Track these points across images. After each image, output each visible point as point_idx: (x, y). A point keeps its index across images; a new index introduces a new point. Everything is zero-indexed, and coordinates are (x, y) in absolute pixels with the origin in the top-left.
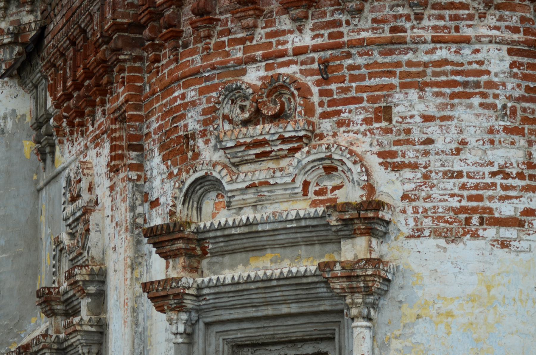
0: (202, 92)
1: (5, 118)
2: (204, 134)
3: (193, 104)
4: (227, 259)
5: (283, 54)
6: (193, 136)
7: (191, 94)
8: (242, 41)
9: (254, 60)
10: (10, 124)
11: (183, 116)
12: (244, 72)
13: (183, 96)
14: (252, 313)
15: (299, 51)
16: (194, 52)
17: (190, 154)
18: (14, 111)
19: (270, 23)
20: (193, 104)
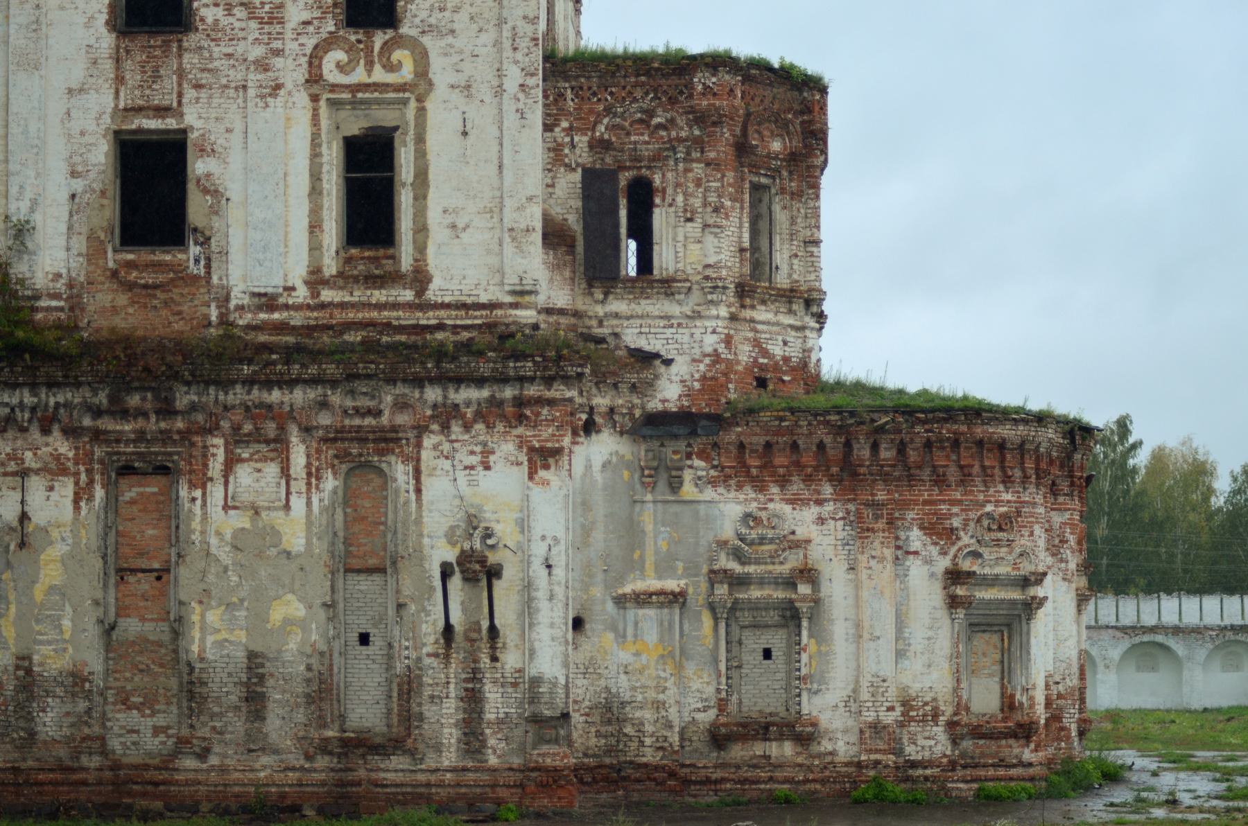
0: (962, 510)
1: (611, 454)
2: (964, 530)
3: (957, 515)
4: (977, 588)
5: (1002, 501)
6: (957, 529)
7: (955, 510)
8: (983, 492)
9: (990, 502)
10: (614, 459)
11: (950, 519)
12: (985, 506)
13: (949, 510)
14: (988, 612)
15: (1009, 502)
16: (956, 490)
17: (954, 537)
18: (617, 452)
19: (996, 487)
20: (957, 515)
